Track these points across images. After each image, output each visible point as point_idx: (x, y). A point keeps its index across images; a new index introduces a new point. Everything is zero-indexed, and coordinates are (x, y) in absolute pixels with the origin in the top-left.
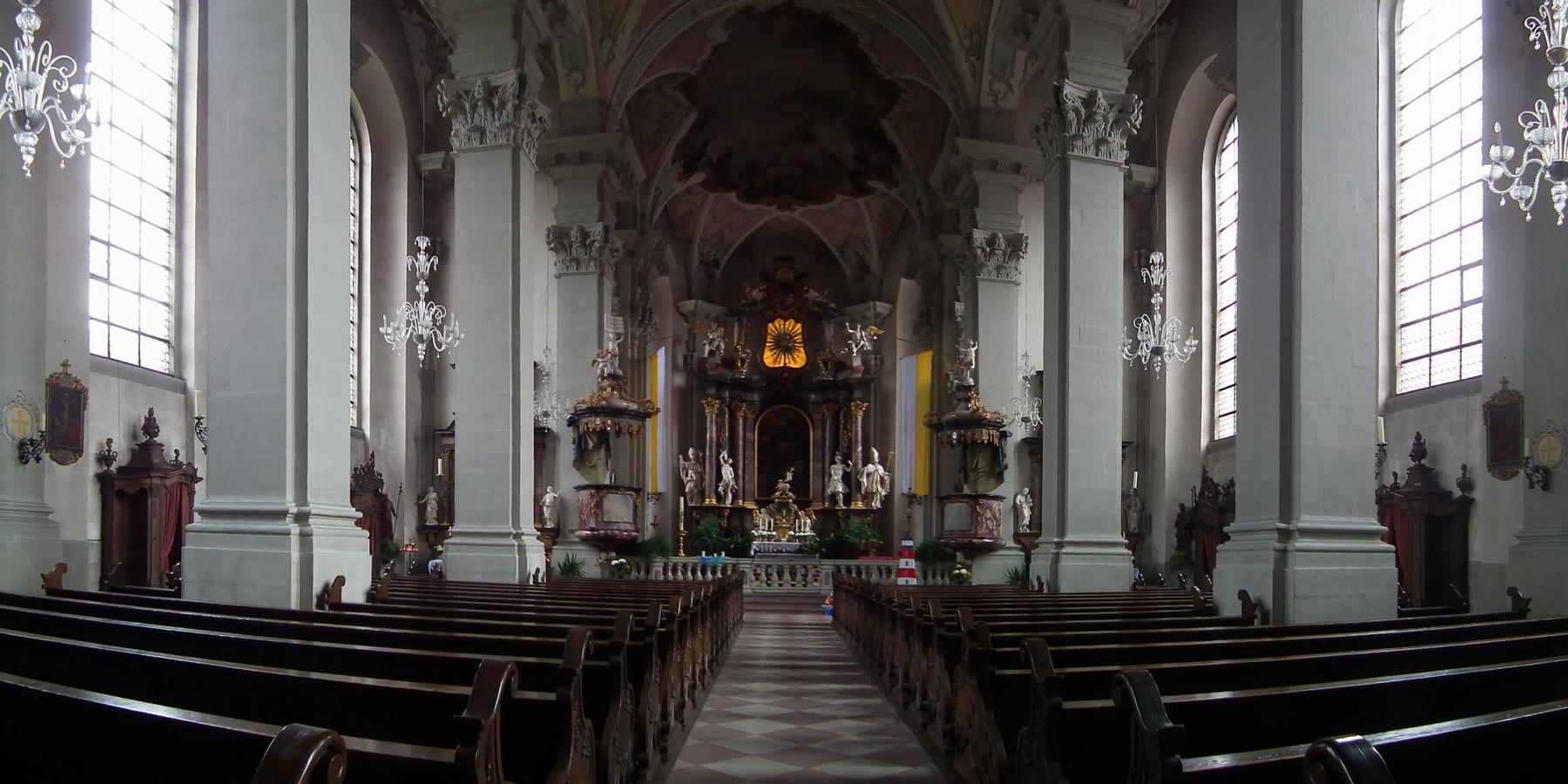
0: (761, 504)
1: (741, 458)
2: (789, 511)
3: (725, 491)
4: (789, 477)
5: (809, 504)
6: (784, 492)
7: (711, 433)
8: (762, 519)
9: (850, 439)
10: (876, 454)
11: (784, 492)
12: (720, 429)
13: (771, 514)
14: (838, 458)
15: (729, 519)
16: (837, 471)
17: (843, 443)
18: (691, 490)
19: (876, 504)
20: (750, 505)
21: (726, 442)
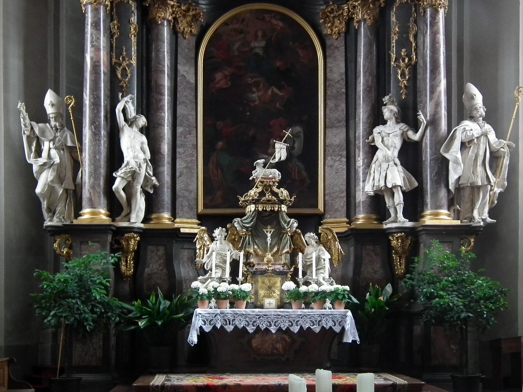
1: (166, 115)
2: (279, 233)
3: (128, 189)
4: (281, 151)
6: (267, 188)
7: (95, 49)
8: (216, 251)
9: (414, 69)
10: (479, 99)
11: (267, 188)
12: (116, 48)
13: (235, 241)
14: (389, 111)
16: (390, 137)
17: (399, 77)
18: (51, 189)
19: (481, 215)
21: (133, 78)
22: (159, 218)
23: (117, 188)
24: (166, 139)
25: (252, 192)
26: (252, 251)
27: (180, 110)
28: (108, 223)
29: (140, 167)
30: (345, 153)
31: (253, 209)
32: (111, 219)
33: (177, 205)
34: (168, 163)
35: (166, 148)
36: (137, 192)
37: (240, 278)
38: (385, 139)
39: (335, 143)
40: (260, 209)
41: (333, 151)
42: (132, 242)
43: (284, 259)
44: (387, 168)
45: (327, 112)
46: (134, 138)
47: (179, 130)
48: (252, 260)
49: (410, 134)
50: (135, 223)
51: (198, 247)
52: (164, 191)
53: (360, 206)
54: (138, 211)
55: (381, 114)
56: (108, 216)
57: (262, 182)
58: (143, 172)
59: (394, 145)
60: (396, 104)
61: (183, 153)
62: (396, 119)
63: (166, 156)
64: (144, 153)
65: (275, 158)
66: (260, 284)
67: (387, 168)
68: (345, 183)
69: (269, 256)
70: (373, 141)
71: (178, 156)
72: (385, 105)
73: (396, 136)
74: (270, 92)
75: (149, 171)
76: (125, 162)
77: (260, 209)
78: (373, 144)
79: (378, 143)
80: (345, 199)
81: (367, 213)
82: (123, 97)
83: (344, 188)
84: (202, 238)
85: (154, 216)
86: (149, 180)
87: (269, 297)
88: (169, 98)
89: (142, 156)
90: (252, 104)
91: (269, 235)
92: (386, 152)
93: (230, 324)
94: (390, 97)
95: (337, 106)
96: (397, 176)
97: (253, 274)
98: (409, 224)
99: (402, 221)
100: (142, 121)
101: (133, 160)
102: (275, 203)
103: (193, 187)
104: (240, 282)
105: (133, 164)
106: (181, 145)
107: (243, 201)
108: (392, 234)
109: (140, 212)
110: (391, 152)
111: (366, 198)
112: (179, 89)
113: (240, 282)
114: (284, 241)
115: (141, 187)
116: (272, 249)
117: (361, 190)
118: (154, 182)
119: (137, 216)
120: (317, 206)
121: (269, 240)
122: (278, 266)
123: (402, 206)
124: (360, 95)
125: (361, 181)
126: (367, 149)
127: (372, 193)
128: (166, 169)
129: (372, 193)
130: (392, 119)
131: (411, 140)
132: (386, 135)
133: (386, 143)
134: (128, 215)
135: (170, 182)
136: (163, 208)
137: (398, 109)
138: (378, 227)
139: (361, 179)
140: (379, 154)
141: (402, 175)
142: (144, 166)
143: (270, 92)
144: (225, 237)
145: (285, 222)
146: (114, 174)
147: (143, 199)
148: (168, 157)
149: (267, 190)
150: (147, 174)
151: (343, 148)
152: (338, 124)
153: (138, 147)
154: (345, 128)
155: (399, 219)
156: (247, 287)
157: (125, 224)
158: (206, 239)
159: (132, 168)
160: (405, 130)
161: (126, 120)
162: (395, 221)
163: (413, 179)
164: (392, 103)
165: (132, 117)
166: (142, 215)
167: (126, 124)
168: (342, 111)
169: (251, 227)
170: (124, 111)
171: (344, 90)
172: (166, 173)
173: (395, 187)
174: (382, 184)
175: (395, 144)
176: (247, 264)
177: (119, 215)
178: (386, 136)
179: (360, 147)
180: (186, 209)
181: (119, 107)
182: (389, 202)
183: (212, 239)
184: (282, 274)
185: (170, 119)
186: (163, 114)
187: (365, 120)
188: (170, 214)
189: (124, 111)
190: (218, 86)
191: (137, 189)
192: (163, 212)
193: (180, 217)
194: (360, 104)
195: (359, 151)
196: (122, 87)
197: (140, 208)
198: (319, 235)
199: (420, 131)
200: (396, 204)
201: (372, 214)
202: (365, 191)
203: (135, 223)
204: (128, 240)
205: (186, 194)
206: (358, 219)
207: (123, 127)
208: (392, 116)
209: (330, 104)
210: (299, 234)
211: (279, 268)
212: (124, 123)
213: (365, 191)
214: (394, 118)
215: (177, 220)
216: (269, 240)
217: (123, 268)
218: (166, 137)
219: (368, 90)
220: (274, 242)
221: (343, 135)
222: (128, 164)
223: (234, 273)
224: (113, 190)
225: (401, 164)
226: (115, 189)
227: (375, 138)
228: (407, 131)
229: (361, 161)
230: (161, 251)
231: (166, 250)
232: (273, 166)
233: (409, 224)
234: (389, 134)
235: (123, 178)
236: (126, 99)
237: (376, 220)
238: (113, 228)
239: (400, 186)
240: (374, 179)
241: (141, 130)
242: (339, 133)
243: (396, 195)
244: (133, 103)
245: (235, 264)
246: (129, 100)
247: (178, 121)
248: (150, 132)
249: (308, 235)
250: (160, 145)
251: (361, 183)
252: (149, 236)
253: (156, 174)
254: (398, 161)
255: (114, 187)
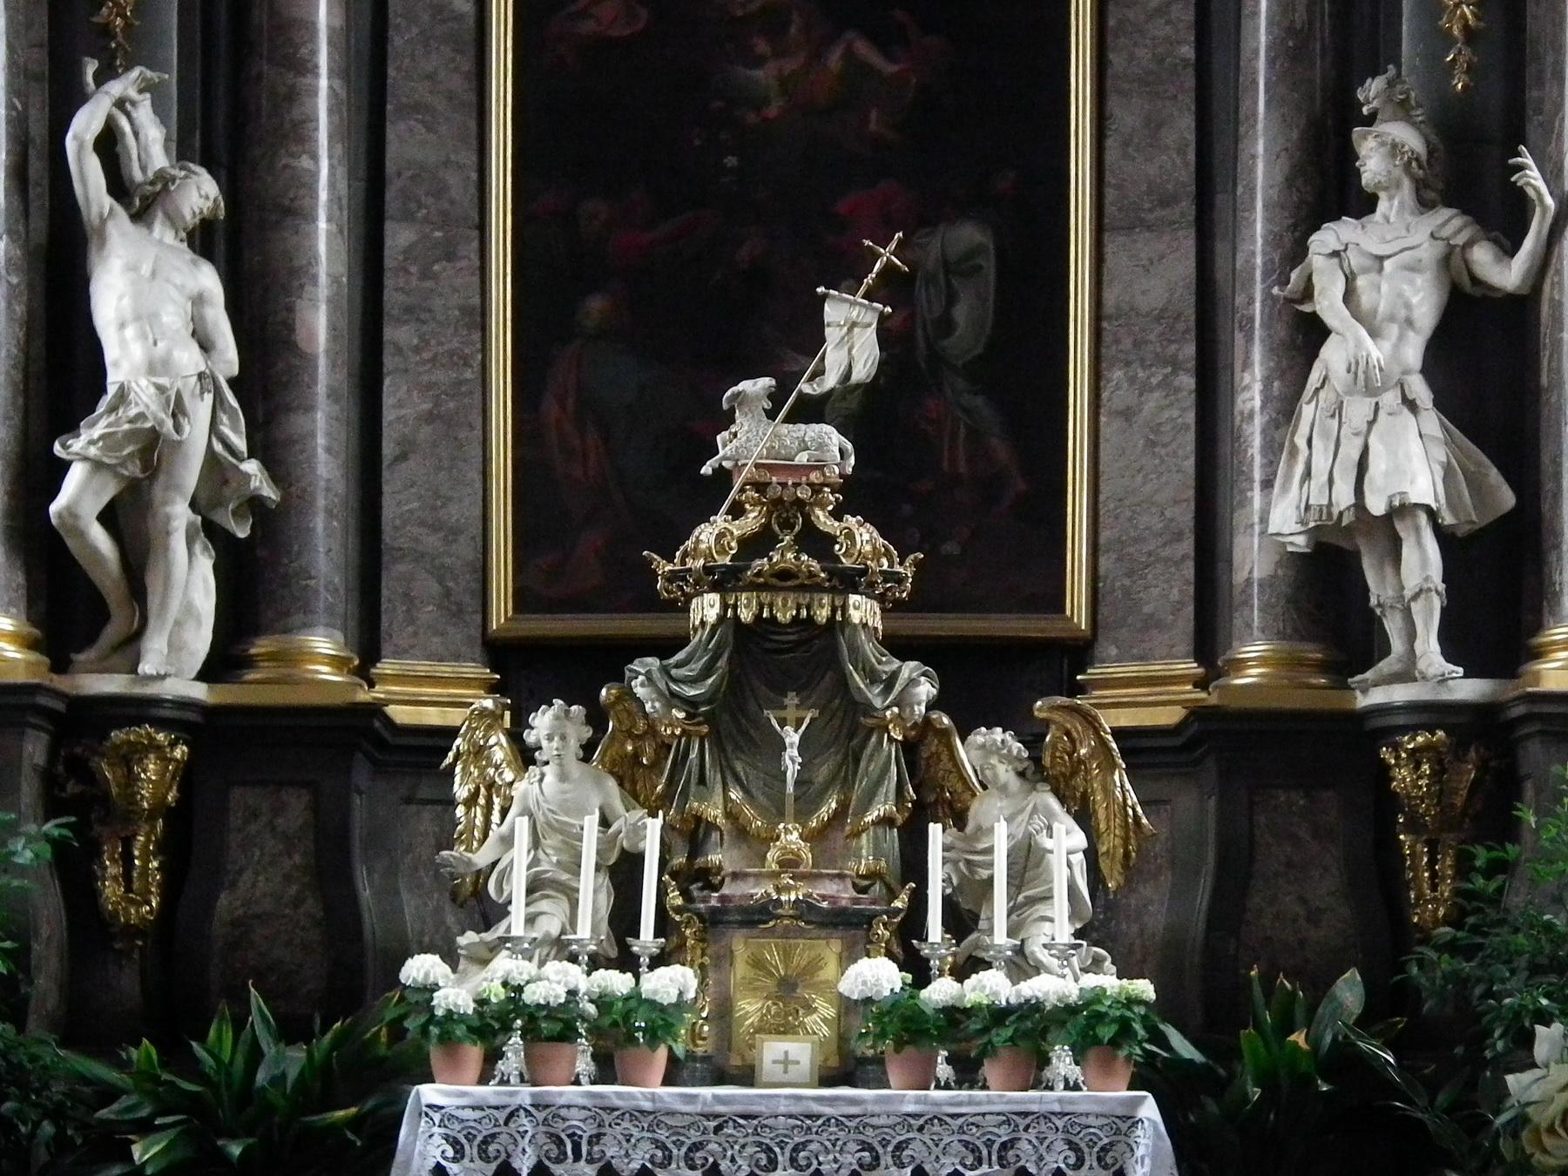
0: (523, 672)
1: (324, 170)
2: (845, 729)
3: (128, 516)
4: (850, 340)
5: (1066, 662)
6: (788, 514)
8: (540, 815)
11: (788, 514)
15: (188, 836)
20: (427, 691)
22: (290, 658)
23: (71, 512)
24: (323, 279)
25: (705, 534)
26: (714, 811)
27: (405, 144)
28: (21, 678)
29: (178, 411)
30: (1190, 350)
31: (712, 615)
32: (46, 660)
33: (385, 592)
34: (333, 394)
35: (319, 323)
36: (168, 533)
37: (647, 938)
38: (1361, 282)
39: (1144, 304)
40: (746, 615)
41: (1137, 344)
42: (151, 769)
43: (870, 852)
44: (1371, 423)
45: (1111, 156)
46: (154, 274)
47: (398, 237)
48: (715, 858)
49: (1483, 257)
50: (161, 677)
51: (461, 791)
52: (310, 531)
53: (1247, 603)
54: (178, 624)
55: (1347, 159)
56: (31, 645)
57: (761, 487)
58: (196, 434)
59: (1403, 313)
60: (1419, 114)
61: (417, 350)
62: (1420, 186)
63: (322, 363)
64: (206, 346)
65: (819, 372)
66: (741, 969)
67: (1371, 423)
68: (1191, 493)
69: (791, 837)
70: (1307, 293)
71: (389, 361)
72: (1370, 120)
73: (1412, 268)
74: (834, 60)
75: (226, 430)
76: (112, 390)
77: (746, 615)
78: (1306, 308)
79: (1329, 304)
80: (1189, 570)
81: (1281, 635)
82: (102, 78)
83: (1185, 515)
84: (480, 752)
85: (261, 646)
86: (229, 475)
87: (784, 1029)
88: (337, 84)
89: (189, 359)
90: (751, 118)
91: (792, 737)
92: (1359, 344)
93: (577, 1156)
94: (1391, 84)
95: (1154, 125)
96: (1413, 462)
97: (705, 919)
98: (1468, 689)
99: (1431, 672)
100: (200, 193)
101: (144, 382)
102: (818, 588)
103: (463, 511)
104: (644, 960)
105: (145, 397)
106: (409, 310)
107: (672, 577)
108: (1388, 734)
109: (190, 626)
110: (1387, 345)
111: (1279, 564)
112: (397, 41)
113: (644, 960)
114: (869, 767)
115: (194, 505)
116: (808, 798)
117: (1257, 528)
118: (254, 483)
119: (175, 647)
120: (1055, 601)
121: (791, 761)
122: (830, 888)
123: (1437, 604)
124: (1255, 72)
125: (1257, 486)
126: (1282, 332)
127: (1301, 540)
128: (322, 429)
129: (1300, 543)
130: (1398, 185)
131: (1491, 288)
132: (1368, 262)
133: (1365, 299)
134: (132, 642)
135: (340, 487)
136: (307, 609)
137: (1428, 143)
138: (1331, 701)
139: (1257, 475)
140: (1333, 356)
141: (1440, 454)
142: (201, 410)
143: (834, 60)
144: (588, 750)
145: (872, 677)
146: (57, 448)
147: (205, 565)
148: (333, 366)
149: (787, 525)
150: (218, 447)
151: (1181, 326)
152: (1159, 213)
153: (174, 318)
154: (1192, 233)
155: (1421, 665)
156: (670, 983)
157: (111, 684)
158: (498, 755)
159: (141, 416)
160: (1460, 240)
161: (119, 187)
162: (1406, 675)
163: (1494, 475)
164: (1403, 110)
165: (150, 174)
166: (200, 641)
167: (119, 209)
168: (1181, 151)
169: (709, 699)
170: (108, 144)
171: (1188, 51)
172: (321, 440)
173: (1401, 510)
174: (1344, 496)
175: (1408, 306)
176: (691, 876)
177: (90, 639)
178: (1366, 271)
179: (1251, 319)
180: (427, 613)
181: (86, 124)
182: (1383, 579)
183: (526, 756)
184: (850, 928)
185: (343, 187)
186: (305, 162)
187: (1274, 193)
188: (339, 636)
189: (108, 144)
190: (588, 27)
191: (168, 518)
192: (307, 626)
193: (399, 654)
194: (1255, 114)
195: (1249, 339)
196: (106, 31)
197: (189, 609)
198: (1033, 742)
199: (1529, 243)
200: (1408, 593)
201: (1303, 639)
202: (1271, 530)
203: (161, 677)
204: (129, 757)
205: (432, 542)
206: (1239, 665)
207: (103, 221)
208: (1398, 172)
209: (1125, 116)
210: (944, 734)
211: (835, 892)
212: (108, 201)
213: (1271, 530)
214: (1407, 184)
215: (386, 667)
216: (791, 761)
217: (111, 891)
218: (322, 271)
219: (1292, 48)
220: (822, 773)
221: (1184, 266)
222: (123, 396)
223: (623, 919)
224: (54, 521)
225: (1438, 404)
226: (60, 516)
227: (1315, 279)
228: (1469, 244)
229: (1258, 387)
230: (297, 808)
231: (315, 808)
232: (809, 411)
233: (1468, 689)
234: (1381, 259)
235: (97, 465)
236: (116, 88)
237: (1323, 667)
238: (43, 700)
239: (1432, 514)
240: (1307, 474)
241: (204, 239)
242: (1162, 257)
243: (1408, 552)
244: (159, 109)
245: (624, 872)
246: (132, 93)
247: (391, 194)
248: (248, 254)
249: (980, 736)
250: (290, 309)
251: (1257, 496)
252: (230, 743)
253: (265, 445)
254: (1420, 389)
255: (54, 508)
